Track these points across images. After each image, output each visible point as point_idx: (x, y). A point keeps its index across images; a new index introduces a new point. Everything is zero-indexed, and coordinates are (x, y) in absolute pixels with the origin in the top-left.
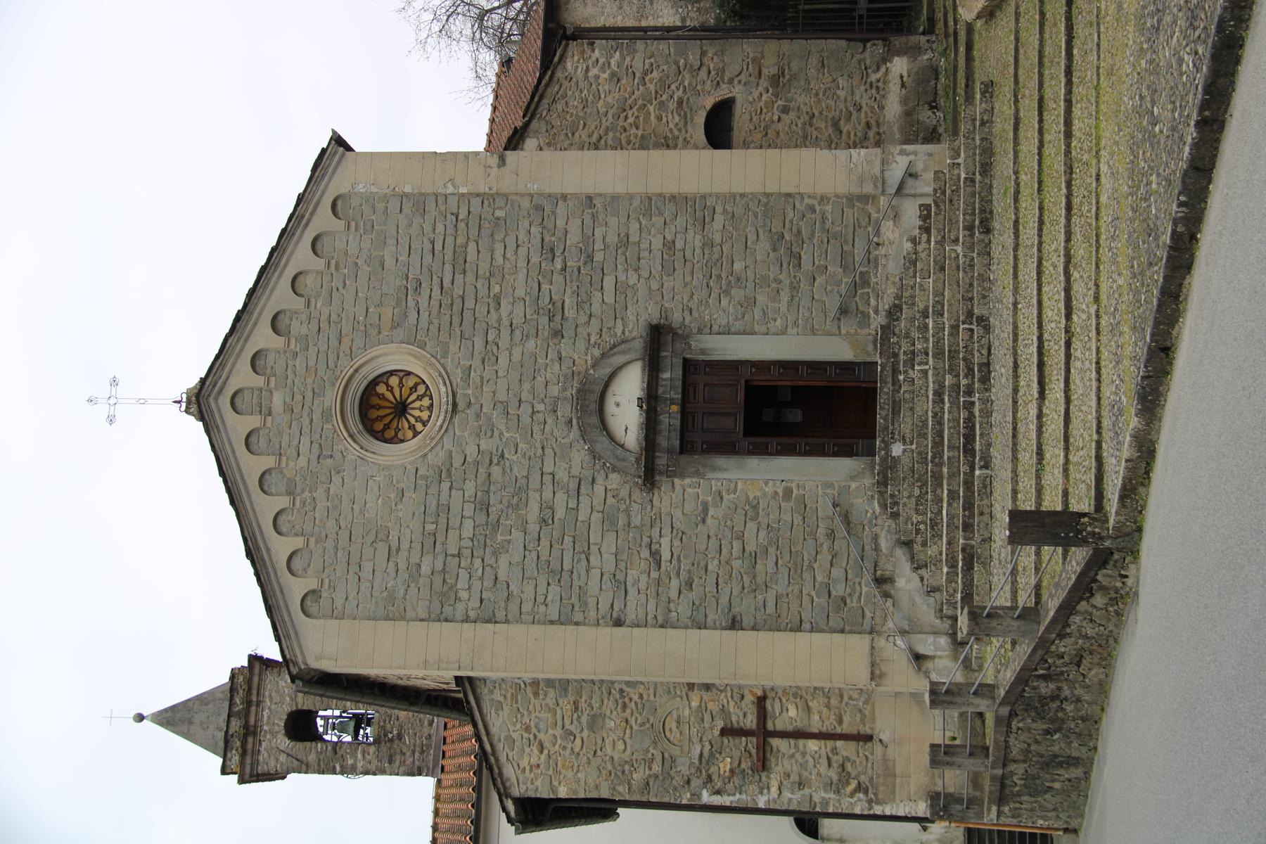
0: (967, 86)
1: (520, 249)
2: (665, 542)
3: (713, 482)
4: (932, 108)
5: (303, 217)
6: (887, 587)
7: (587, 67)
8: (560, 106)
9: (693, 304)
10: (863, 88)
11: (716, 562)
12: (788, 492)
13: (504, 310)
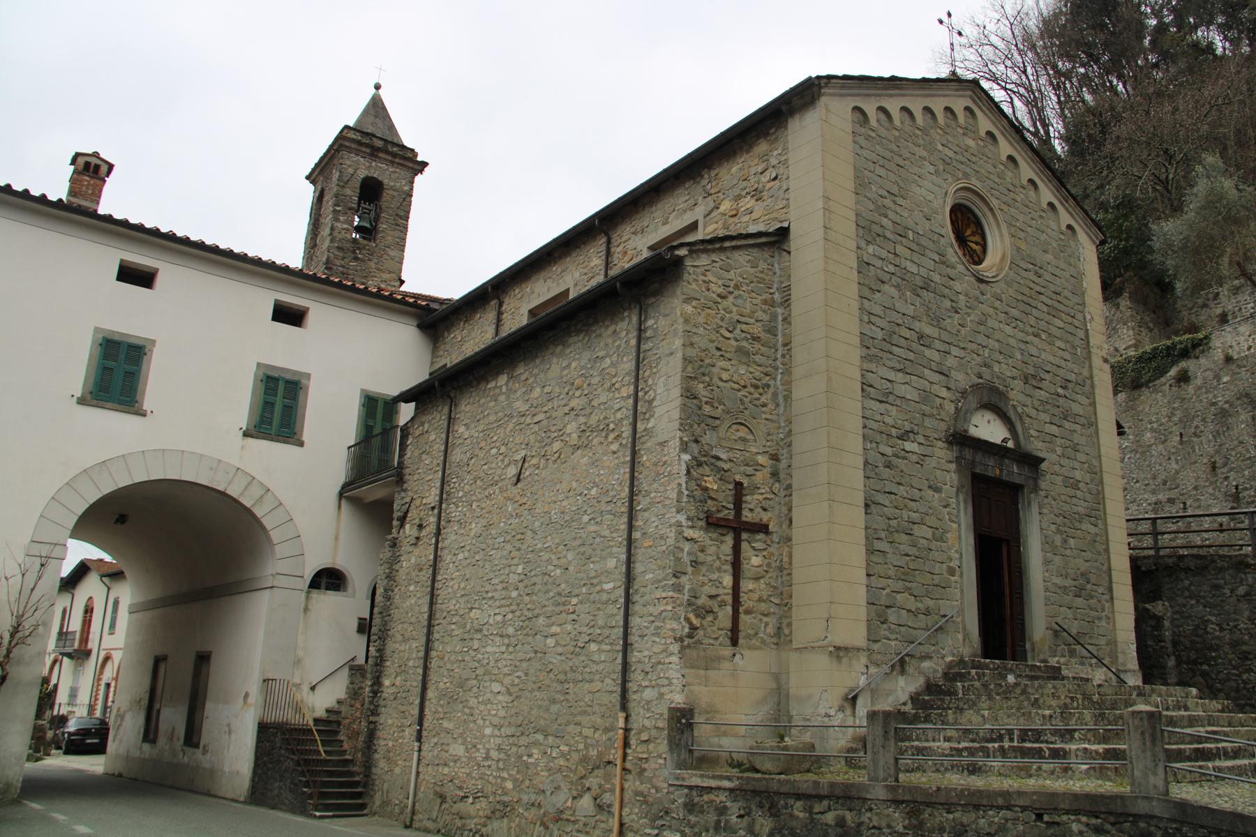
6: (898, 668)
12: (952, 572)
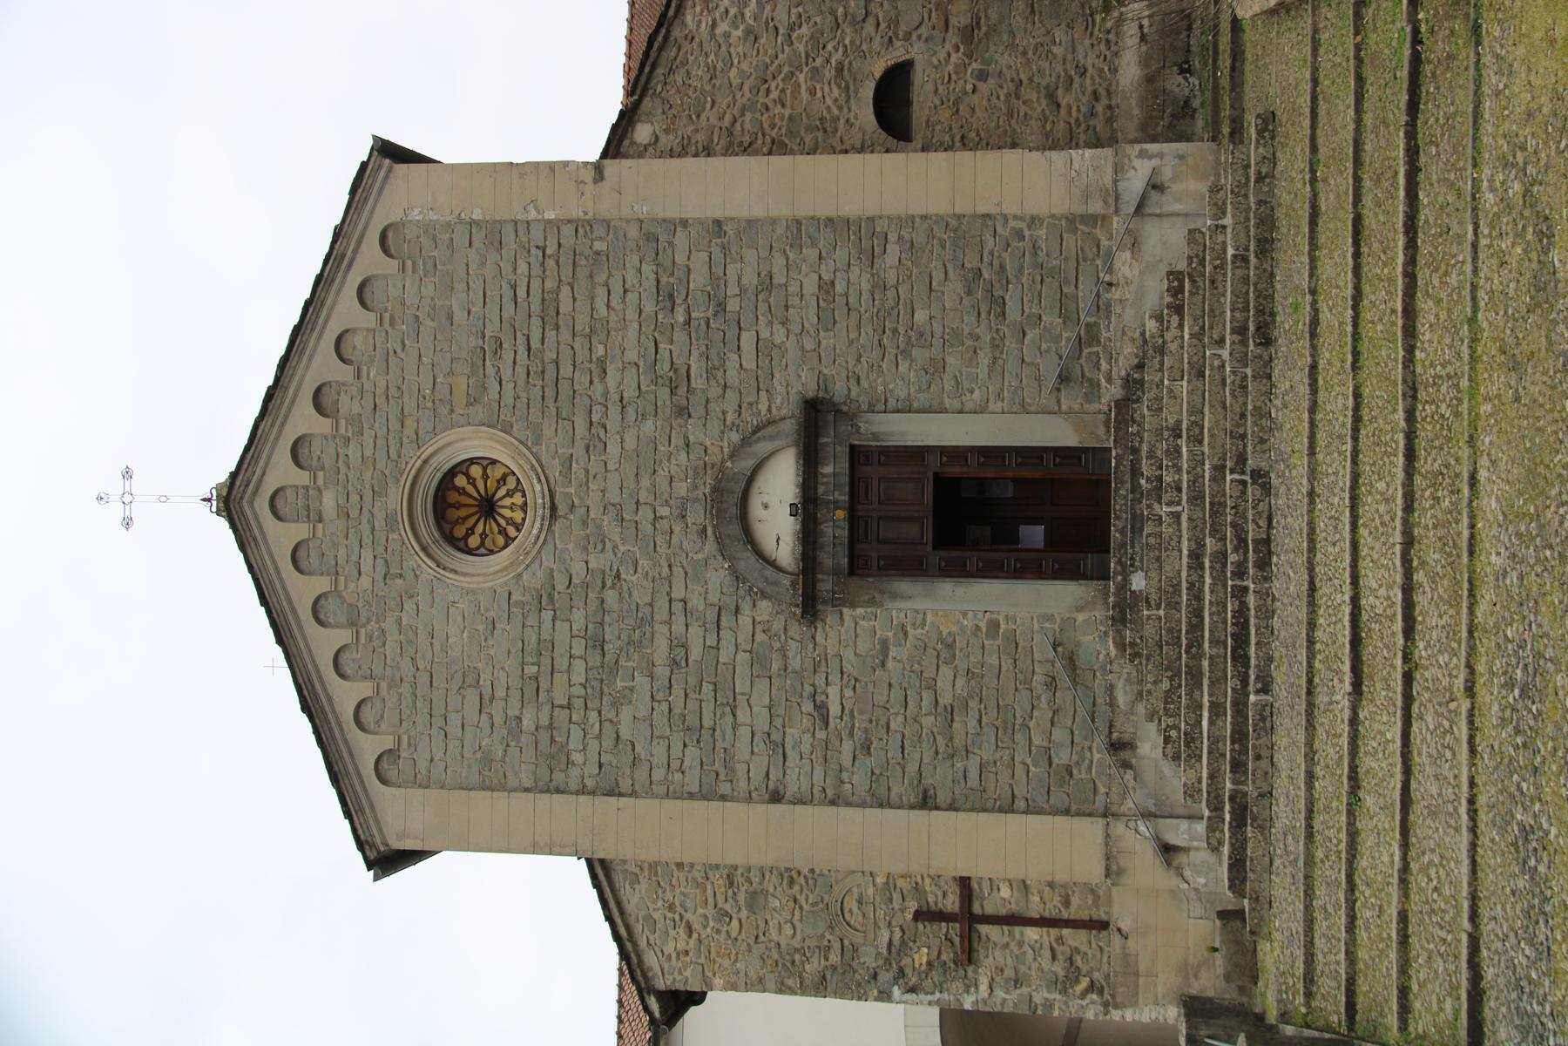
0: (1233, 68)
1: (629, 295)
2: (833, 691)
3: (894, 613)
4: (1183, 71)
5: (343, 256)
6: (1126, 754)
7: (714, 21)
8: (679, 78)
9: (861, 370)
10: (1087, 42)
11: (900, 718)
12: (994, 626)
13: (612, 380)
